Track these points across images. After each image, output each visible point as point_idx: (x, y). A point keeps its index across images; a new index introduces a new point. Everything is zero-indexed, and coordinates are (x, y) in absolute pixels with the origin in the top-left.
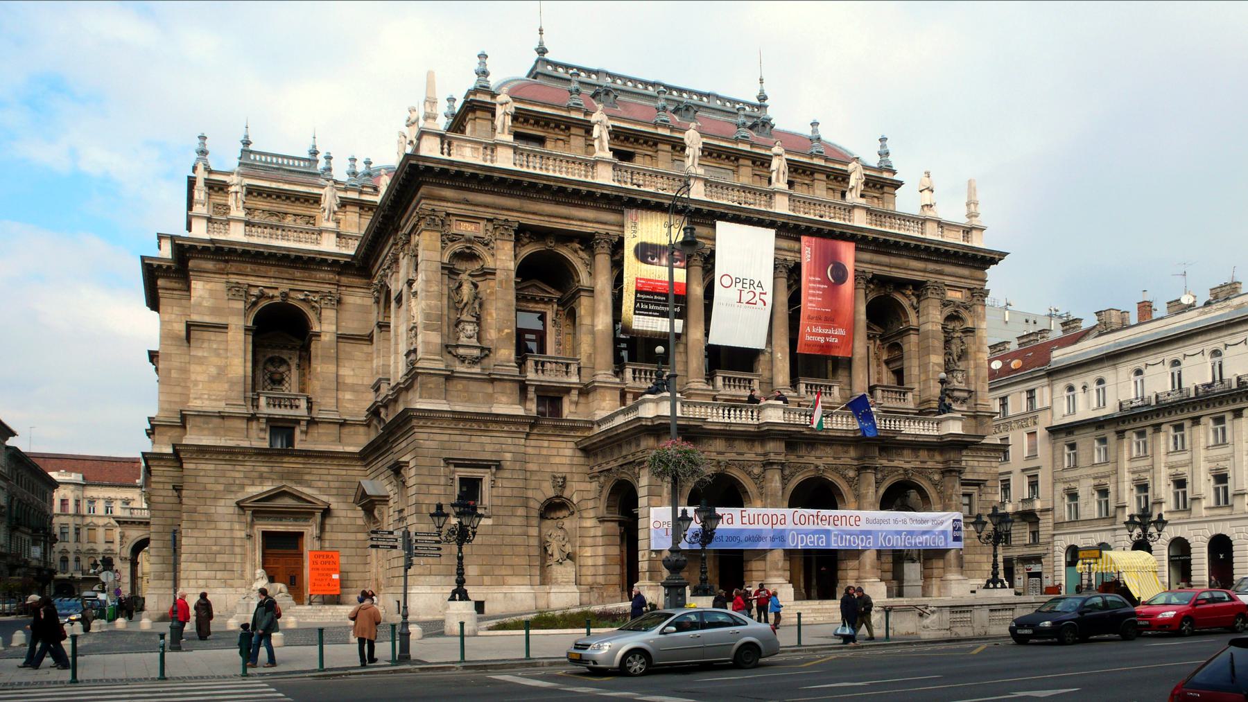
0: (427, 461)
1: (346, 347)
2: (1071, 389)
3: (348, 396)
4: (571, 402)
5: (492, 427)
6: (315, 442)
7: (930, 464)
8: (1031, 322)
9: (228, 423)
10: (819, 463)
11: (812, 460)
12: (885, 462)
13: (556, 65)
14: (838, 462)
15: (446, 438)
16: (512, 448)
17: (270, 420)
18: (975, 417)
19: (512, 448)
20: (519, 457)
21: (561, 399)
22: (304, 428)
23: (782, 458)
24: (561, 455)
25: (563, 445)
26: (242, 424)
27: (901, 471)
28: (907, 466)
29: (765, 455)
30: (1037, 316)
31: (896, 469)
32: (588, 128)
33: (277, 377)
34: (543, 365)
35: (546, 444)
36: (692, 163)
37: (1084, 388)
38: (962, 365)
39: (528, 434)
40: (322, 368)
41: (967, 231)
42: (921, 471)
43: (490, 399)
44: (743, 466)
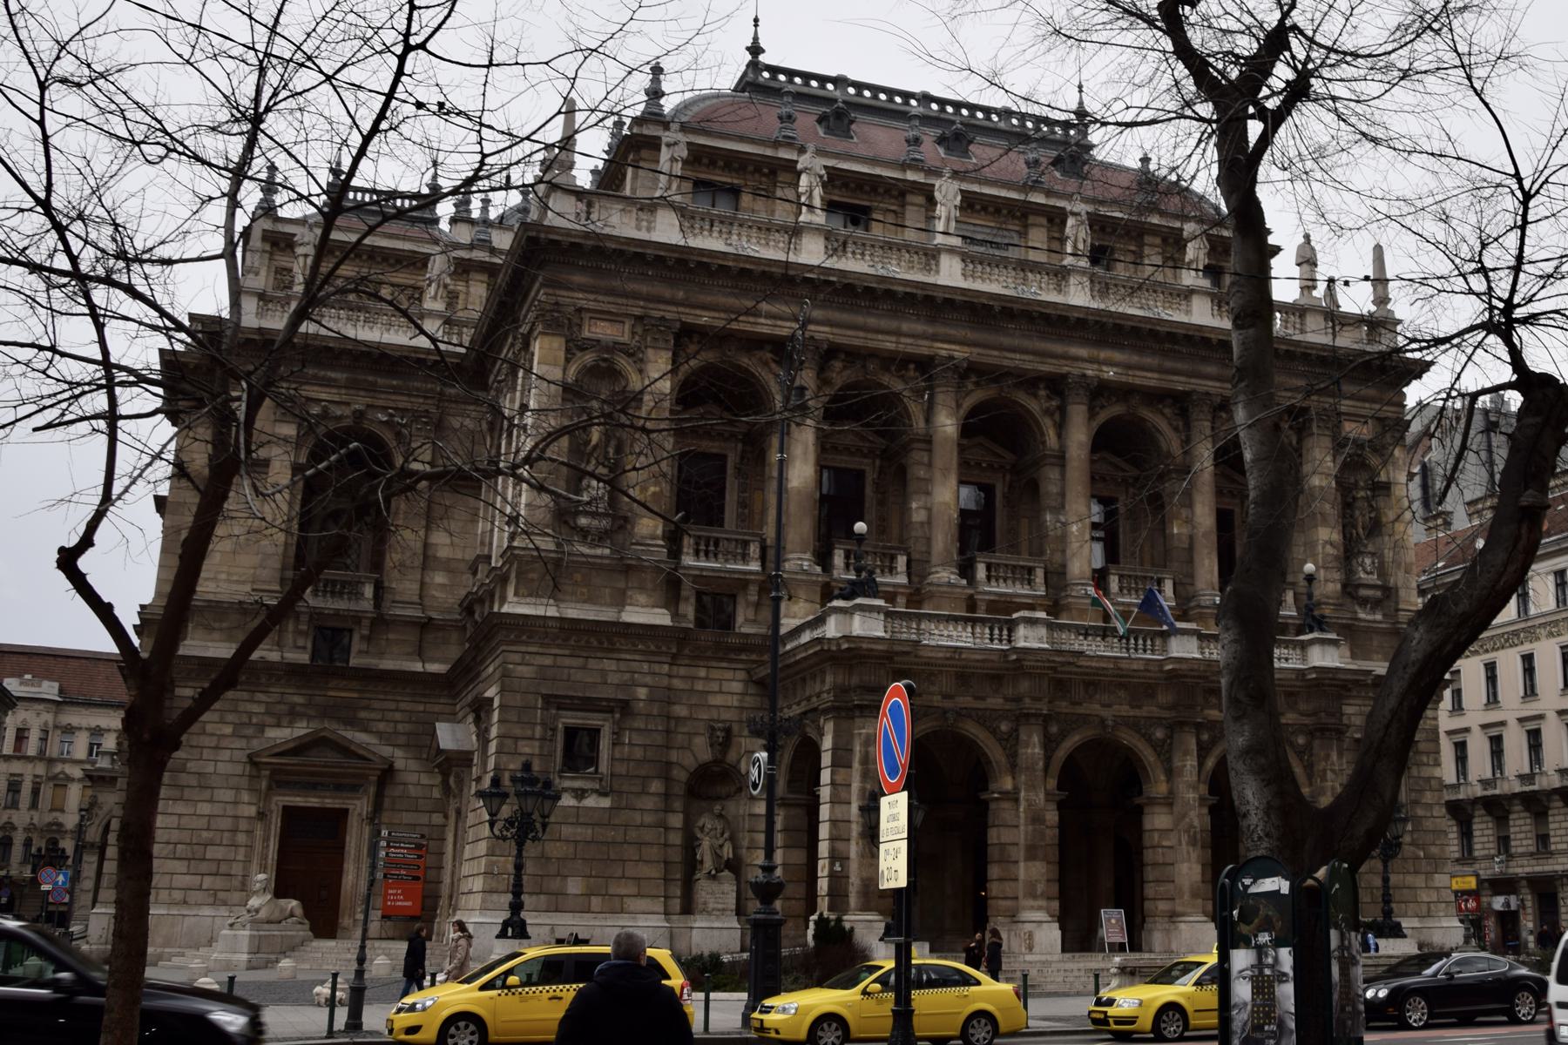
4: (748, 604)
6: (381, 655)
16: (648, 680)
19: (648, 680)
21: (733, 597)
22: (366, 632)
24: (726, 691)
34: (716, 544)
35: (702, 673)
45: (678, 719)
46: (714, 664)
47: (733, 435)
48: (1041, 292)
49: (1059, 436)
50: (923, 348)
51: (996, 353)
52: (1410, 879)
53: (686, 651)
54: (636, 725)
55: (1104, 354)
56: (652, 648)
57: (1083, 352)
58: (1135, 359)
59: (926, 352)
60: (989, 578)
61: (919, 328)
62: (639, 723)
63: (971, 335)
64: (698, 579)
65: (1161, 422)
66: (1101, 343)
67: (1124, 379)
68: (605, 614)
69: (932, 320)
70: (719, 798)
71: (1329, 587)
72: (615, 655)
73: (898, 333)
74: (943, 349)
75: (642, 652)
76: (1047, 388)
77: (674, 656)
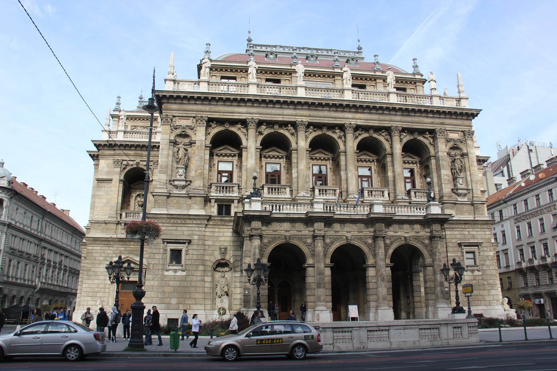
5: (188, 221)
7: (422, 233)
9: (108, 226)
10: (349, 235)
11: (345, 233)
12: (390, 233)
13: (256, 45)
14: (361, 234)
18: (472, 204)
19: (198, 233)
20: (201, 238)
23: (322, 233)
24: (225, 235)
26: (114, 226)
27: (403, 239)
28: (406, 235)
31: (400, 237)
35: (217, 230)
36: (252, 77)
38: (462, 175)
39: (206, 225)
41: (459, 100)
42: (417, 238)
43: (189, 207)
44: (300, 238)
46: (221, 227)
48: (335, 96)
49: (345, 145)
50: (292, 119)
52: (481, 292)
53: (211, 223)
54: (194, 248)
55: (358, 116)
56: (199, 222)
59: (293, 120)
61: (291, 112)
64: (217, 200)
65: (382, 138)
67: (365, 124)
68: (185, 212)
71: (447, 189)
74: (299, 119)
76: (339, 129)
77: (206, 225)
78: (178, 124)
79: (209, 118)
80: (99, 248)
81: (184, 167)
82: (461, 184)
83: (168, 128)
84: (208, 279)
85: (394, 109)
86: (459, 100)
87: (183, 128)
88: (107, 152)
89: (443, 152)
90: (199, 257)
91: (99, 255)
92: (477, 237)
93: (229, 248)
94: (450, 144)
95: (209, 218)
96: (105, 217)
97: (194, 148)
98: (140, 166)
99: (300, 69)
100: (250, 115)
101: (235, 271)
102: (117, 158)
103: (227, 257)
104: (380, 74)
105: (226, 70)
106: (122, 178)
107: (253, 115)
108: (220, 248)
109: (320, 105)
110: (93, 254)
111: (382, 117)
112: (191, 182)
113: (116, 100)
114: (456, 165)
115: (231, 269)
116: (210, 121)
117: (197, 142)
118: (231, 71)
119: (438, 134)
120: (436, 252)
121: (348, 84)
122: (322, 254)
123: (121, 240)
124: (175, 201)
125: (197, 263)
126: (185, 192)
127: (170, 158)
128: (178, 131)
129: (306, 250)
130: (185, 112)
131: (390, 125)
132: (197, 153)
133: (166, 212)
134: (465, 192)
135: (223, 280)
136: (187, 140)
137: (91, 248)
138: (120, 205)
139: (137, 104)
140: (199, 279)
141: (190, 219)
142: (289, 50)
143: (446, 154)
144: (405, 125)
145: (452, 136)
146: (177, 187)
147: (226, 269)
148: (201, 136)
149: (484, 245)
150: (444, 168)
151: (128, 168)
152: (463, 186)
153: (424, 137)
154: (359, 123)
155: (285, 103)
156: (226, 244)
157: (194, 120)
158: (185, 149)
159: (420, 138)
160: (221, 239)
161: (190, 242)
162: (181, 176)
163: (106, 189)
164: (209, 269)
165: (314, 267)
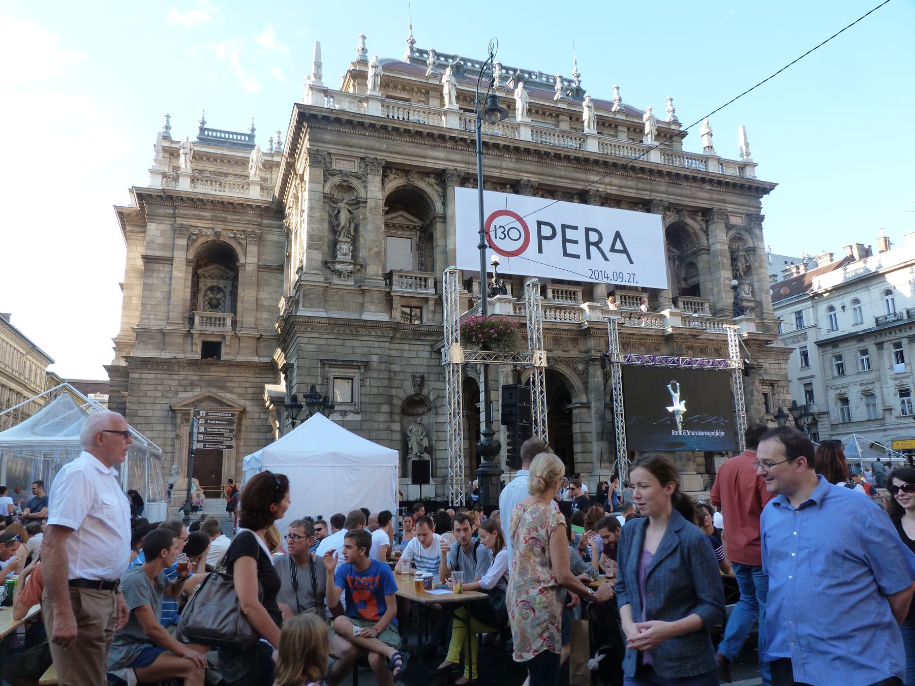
0: (306, 363)
1: (266, 275)
2: (832, 309)
3: (265, 315)
8: (789, 263)
13: (422, 52)
15: (323, 342)
17: (202, 334)
19: (378, 351)
25: (421, 348)
29: (587, 352)
30: (792, 258)
32: (439, 89)
33: (214, 302)
35: (407, 347)
37: (843, 307)
40: (246, 294)
43: (362, 307)
45: (395, 372)
47: (414, 228)
51: (552, 179)
53: (398, 336)
55: (607, 180)
57: (595, 178)
58: (623, 182)
60: (554, 297)
61: (512, 165)
62: (374, 374)
63: (539, 170)
66: (607, 174)
67: (618, 193)
68: (355, 316)
69: (518, 161)
70: (418, 415)
72: (360, 338)
73: (502, 168)
75: (375, 336)
77: (392, 338)
78: (334, 167)
79: (387, 162)
80: (152, 376)
81: (349, 240)
82: (745, 292)
83: (319, 172)
84: (396, 427)
85: (660, 173)
86: (743, 167)
87: (346, 175)
88: (161, 211)
89: (724, 244)
90: (381, 391)
91: (152, 387)
92: (770, 371)
93: (426, 376)
94: (732, 233)
95: (395, 327)
96: (159, 323)
97: (363, 211)
98: (222, 239)
99: (520, 96)
100: (451, 164)
101: (437, 414)
102: (179, 221)
103: (425, 392)
104: (624, 118)
105: (396, 87)
106: (191, 257)
107: (456, 164)
108: (414, 377)
109: (557, 157)
110: (142, 387)
111: (641, 185)
112: (362, 266)
113: (164, 123)
114: (740, 264)
115: (430, 410)
116: (388, 169)
117: (369, 201)
118: (404, 89)
119: (715, 217)
120: (752, 391)
121: (589, 127)
122: (603, 387)
123: (192, 363)
124: (337, 298)
125: (378, 401)
126: (353, 283)
127: (326, 225)
128: (336, 180)
129: (575, 381)
130: (347, 148)
131: (652, 197)
132: (369, 219)
133: (324, 315)
134: (753, 304)
135: (420, 429)
136: (348, 197)
137: (137, 376)
138: (188, 303)
139: (197, 132)
140: (382, 426)
141: (365, 327)
142: (473, 66)
143: (727, 247)
144: (673, 199)
145: (735, 220)
146: (339, 274)
147: (420, 410)
148: (375, 191)
149: (781, 383)
150: (724, 268)
151: (201, 240)
152: (750, 297)
153: (694, 219)
154: (609, 191)
155: (506, 148)
156: (422, 370)
157: (363, 165)
158: (349, 211)
159: (689, 221)
160: (413, 362)
161: (366, 365)
162: (345, 255)
163: (162, 275)
164: (397, 410)
165: (589, 408)
